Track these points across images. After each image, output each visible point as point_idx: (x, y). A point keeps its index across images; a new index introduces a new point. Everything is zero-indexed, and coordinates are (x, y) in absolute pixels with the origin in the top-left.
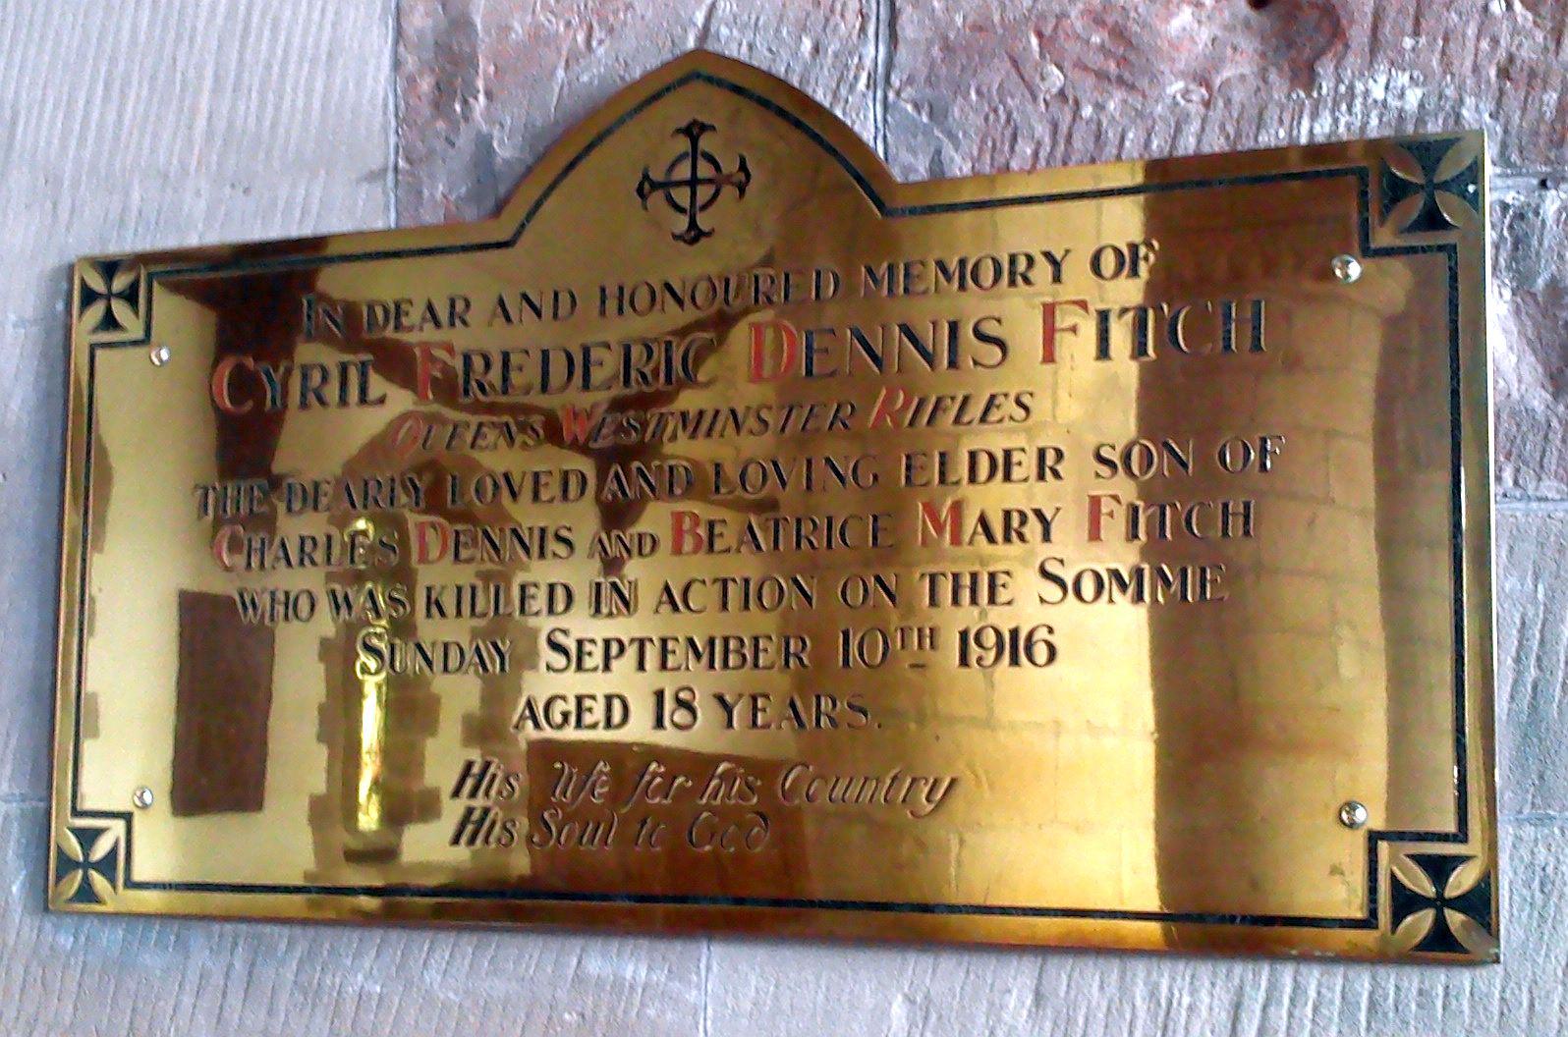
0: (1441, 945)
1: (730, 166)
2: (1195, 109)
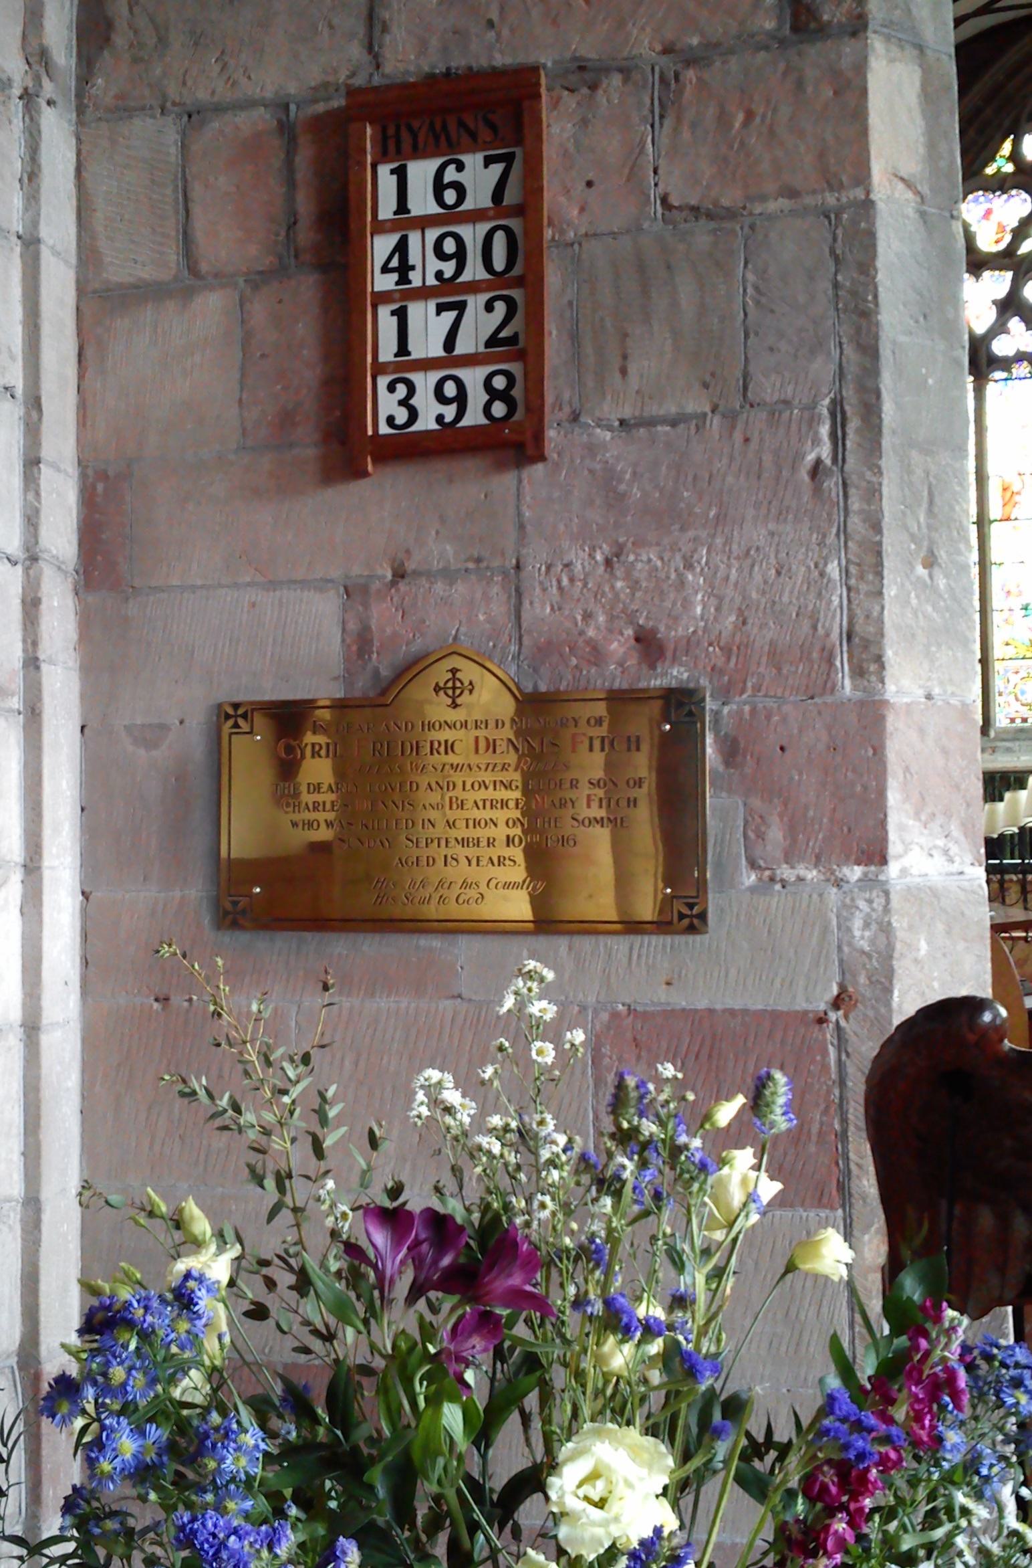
0: (692, 929)
1: (466, 683)
2: (618, 673)
